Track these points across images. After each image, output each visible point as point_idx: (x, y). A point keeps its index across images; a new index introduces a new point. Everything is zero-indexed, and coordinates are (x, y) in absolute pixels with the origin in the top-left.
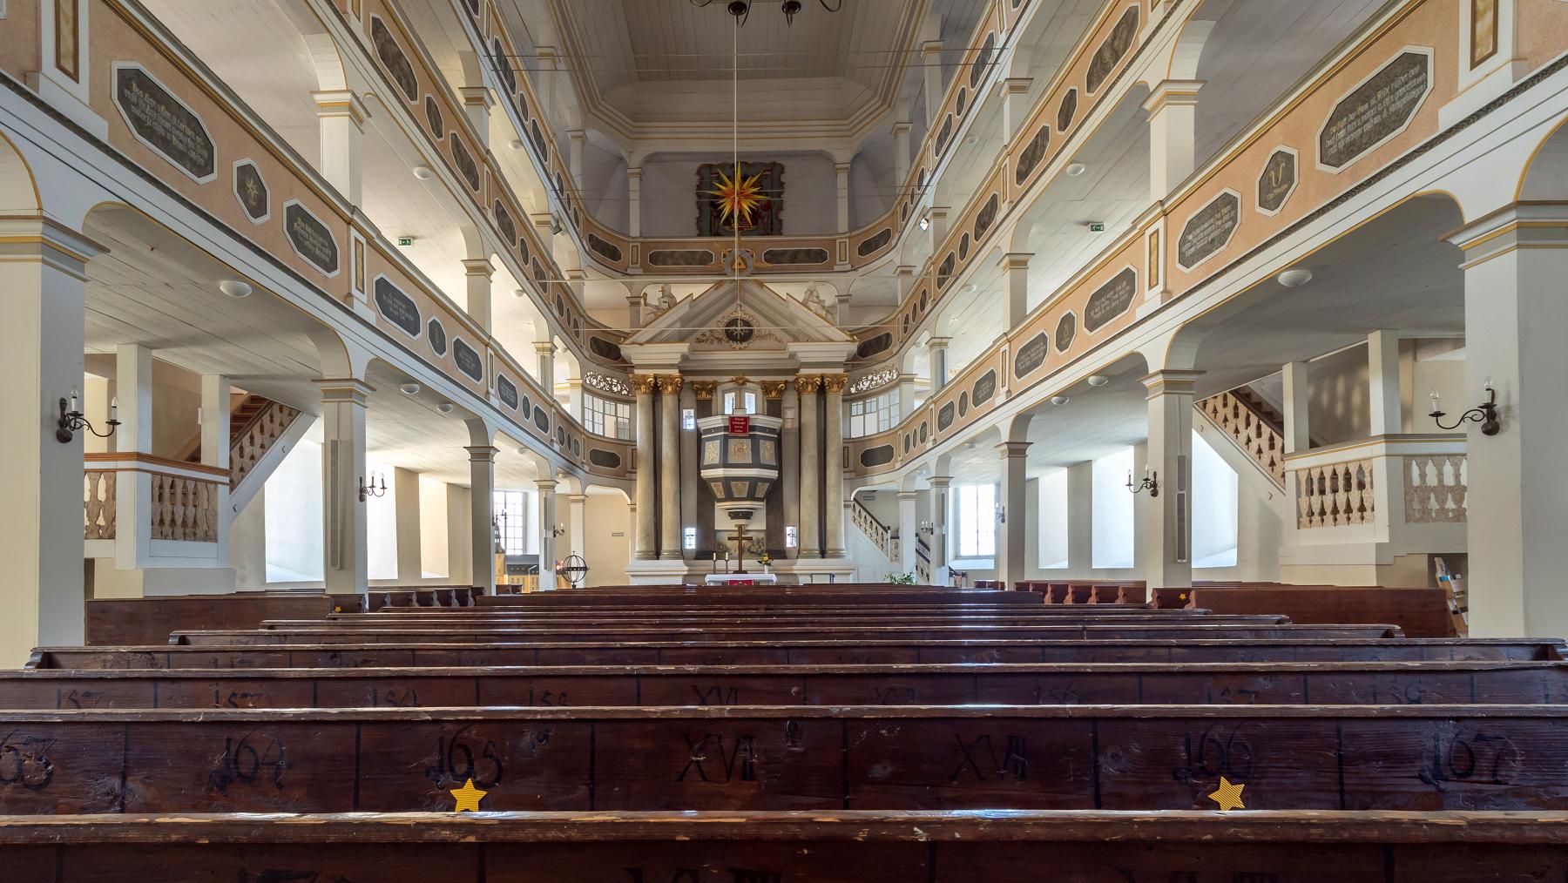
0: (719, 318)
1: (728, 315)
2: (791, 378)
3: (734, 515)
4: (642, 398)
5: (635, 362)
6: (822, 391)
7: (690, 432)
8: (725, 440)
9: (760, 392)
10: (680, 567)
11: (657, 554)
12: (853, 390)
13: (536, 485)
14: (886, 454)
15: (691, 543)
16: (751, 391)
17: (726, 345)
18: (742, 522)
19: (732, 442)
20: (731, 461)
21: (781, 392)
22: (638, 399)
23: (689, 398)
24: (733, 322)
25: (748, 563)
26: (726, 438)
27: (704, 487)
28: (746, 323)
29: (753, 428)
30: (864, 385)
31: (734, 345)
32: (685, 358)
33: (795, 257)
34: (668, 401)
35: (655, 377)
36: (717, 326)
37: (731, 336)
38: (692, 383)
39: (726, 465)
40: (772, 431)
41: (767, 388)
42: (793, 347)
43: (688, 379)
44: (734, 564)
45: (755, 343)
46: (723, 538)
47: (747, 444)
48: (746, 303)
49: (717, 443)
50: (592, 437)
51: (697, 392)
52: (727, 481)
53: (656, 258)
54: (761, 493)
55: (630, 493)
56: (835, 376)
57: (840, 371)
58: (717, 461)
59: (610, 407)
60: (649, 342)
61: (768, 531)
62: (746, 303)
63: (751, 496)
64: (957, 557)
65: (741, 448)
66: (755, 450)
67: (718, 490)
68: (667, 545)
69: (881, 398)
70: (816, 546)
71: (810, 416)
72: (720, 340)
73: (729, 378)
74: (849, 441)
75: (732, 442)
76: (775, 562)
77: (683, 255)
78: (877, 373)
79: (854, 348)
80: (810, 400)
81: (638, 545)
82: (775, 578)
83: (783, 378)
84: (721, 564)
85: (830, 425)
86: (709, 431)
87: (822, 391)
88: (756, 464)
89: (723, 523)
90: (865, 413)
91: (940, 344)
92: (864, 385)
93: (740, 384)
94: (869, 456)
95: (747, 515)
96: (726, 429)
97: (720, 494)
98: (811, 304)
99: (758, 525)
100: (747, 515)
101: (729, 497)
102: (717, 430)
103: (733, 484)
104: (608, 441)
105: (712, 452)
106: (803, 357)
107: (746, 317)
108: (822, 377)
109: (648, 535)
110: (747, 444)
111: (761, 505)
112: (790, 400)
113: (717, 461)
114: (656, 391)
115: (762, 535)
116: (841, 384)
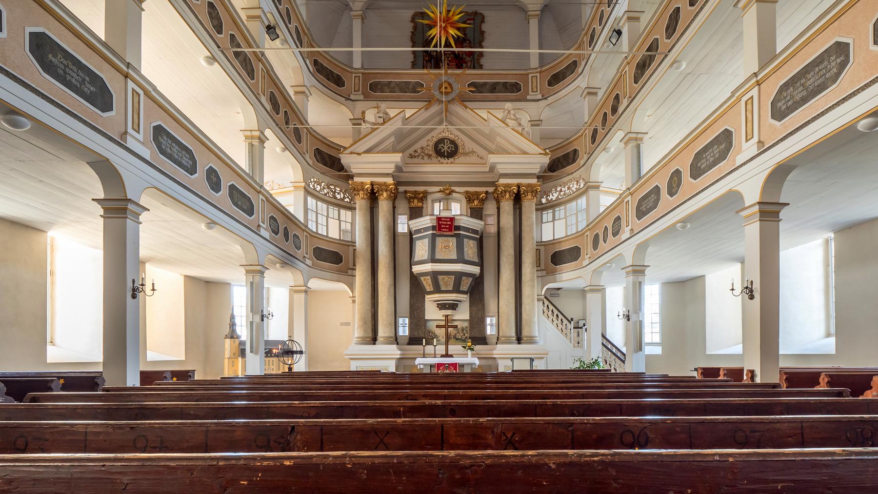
0: (429, 137)
1: (435, 136)
2: (491, 189)
3: (442, 306)
4: (361, 203)
5: (354, 171)
6: (518, 199)
8: (433, 238)
9: (464, 201)
10: (394, 351)
11: (374, 340)
12: (544, 201)
14: (574, 254)
15: (404, 331)
16: (456, 200)
17: (435, 160)
18: (449, 312)
20: (438, 257)
21: (482, 201)
22: (357, 206)
23: (402, 206)
24: (441, 141)
25: (454, 348)
27: (415, 280)
28: (453, 142)
29: (458, 228)
30: (553, 196)
31: (442, 160)
32: (399, 169)
33: (494, 88)
34: (384, 205)
35: (372, 184)
36: (427, 142)
37: (439, 153)
38: (406, 192)
40: (475, 232)
41: (470, 198)
42: (493, 159)
43: (401, 189)
44: (441, 349)
45: (460, 159)
46: (432, 326)
47: (452, 242)
49: (426, 241)
51: (409, 200)
52: (435, 275)
53: (374, 87)
54: (465, 286)
55: (351, 287)
56: (529, 185)
57: (534, 181)
58: (426, 257)
59: (333, 211)
60: (368, 151)
61: (471, 321)
63: (457, 290)
65: (447, 246)
66: (460, 248)
68: (383, 331)
69: (569, 206)
70: (514, 334)
71: (508, 220)
72: (430, 156)
73: (437, 189)
74: (540, 243)
76: (478, 348)
77: (398, 84)
78: (565, 184)
79: (546, 160)
80: (507, 206)
81: (357, 331)
82: (477, 361)
83: (484, 189)
84: (429, 349)
85: (525, 228)
86: (418, 231)
87: (518, 199)
88: (461, 260)
89: (433, 313)
90: (554, 219)
91: (636, 139)
92: (553, 196)
93: (448, 193)
94: (557, 257)
95: (453, 306)
96: (434, 228)
98: (508, 121)
99: (463, 315)
100: (453, 306)
101: (437, 290)
102: (426, 229)
103: (440, 277)
104: (332, 241)
105: (422, 249)
106: (501, 169)
107: (451, 137)
108: (519, 186)
109: (365, 323)
110: (452, 242)
111: (465, 298)
112: (490, 208)
113: (426, 257)
114: (373, 197)
116: (535, 192)
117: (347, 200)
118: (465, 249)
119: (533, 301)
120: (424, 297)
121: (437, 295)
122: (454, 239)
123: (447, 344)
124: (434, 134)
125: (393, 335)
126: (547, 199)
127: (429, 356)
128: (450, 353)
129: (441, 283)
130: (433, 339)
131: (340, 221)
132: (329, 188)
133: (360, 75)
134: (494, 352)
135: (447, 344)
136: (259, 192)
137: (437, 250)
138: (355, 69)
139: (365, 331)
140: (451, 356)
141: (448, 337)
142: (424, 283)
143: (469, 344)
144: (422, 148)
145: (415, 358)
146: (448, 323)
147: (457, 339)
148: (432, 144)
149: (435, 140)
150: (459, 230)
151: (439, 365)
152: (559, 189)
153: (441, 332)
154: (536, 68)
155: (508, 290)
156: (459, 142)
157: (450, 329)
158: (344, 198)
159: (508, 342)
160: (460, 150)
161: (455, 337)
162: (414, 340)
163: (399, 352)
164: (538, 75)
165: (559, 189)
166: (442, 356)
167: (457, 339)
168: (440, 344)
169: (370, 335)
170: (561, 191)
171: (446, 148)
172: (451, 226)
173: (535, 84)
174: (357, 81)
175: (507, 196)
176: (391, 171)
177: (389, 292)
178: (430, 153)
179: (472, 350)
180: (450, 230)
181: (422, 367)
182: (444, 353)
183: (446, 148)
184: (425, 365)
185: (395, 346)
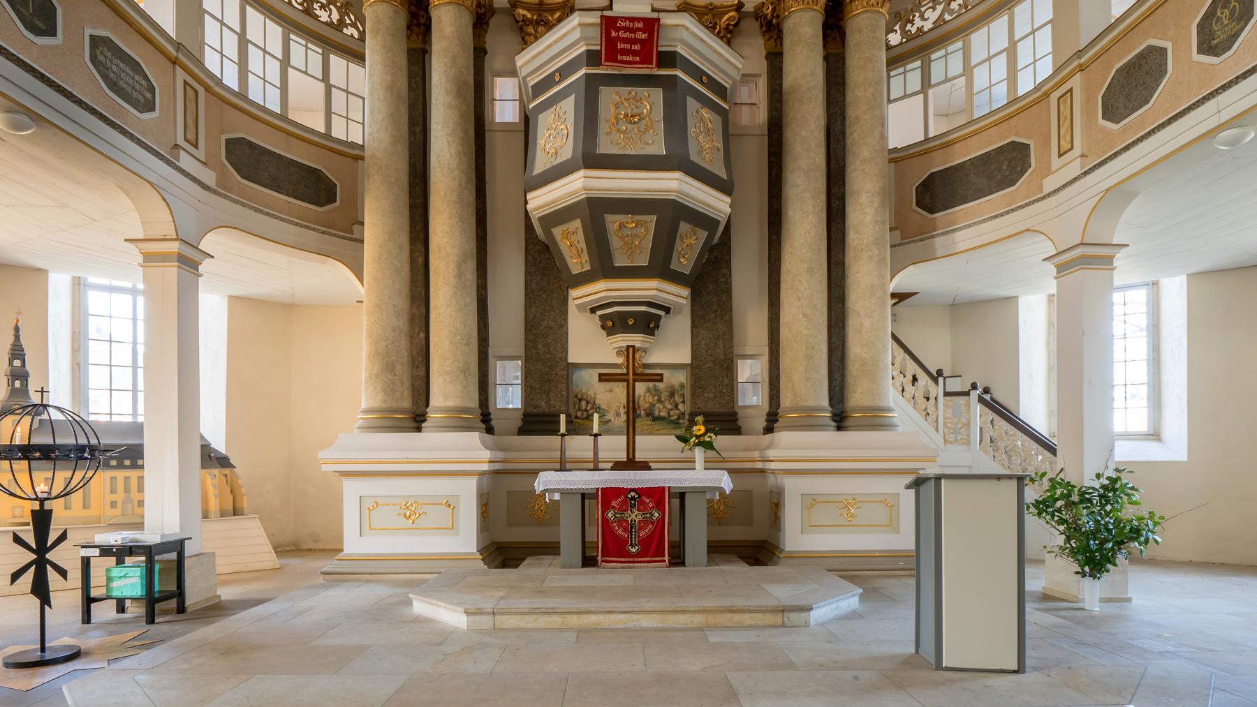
7: (507, 128)
13: (134, 255)
14: (1005, 166)
18: (637, 339)
19: (609, 97)
25: (651, 444)
39: (592, 159)
44: (613, 446)
50: (237, 103)
54: (684, 262)
64: (1155, 435)
69: (978, 38)
70: (822, 399)
75: (609, 97)
76: (721, 441)
84: (579, 445)
90: (926, 84)
94: (936, 190)
95: (646, 321)
97: (577, 262)
100: (646, 321)
102: (565, 71)
104: (302, 135)
109: (389, 368)
111: (677, 295)
115: (680, 378)
118: (692, 130)
120: (565, 301)
121: (601, 285)
123: (631, 431)
125: (474, 403)
126: (904, 33)
128: (639, 456)
130: (589, 418)
131: (329, 88)
134: (771, 454)
135: (631, 431)
136: (175, 62)
137: (603, 127)
139: (389, 390)
140: (645, 466)
141: (632, 407)
143: (699, 429)
145: (535, 473)
146: (633, 372)
151: (609, 495)
153: (612, 397)
157: (640, 388)
158: (341, 23)
159: (807, 423)
161: (649, 414)
162: (536, 422)
163: (487, 454)
166: (618, 466)
168: (610, 432)
169: (407, 403)
172: (648, 45)
177: (459, 275)
179: (709, 446)
181: (557, 497)
182: (623, 456)
184: (564, 493)
185: (474, 438)
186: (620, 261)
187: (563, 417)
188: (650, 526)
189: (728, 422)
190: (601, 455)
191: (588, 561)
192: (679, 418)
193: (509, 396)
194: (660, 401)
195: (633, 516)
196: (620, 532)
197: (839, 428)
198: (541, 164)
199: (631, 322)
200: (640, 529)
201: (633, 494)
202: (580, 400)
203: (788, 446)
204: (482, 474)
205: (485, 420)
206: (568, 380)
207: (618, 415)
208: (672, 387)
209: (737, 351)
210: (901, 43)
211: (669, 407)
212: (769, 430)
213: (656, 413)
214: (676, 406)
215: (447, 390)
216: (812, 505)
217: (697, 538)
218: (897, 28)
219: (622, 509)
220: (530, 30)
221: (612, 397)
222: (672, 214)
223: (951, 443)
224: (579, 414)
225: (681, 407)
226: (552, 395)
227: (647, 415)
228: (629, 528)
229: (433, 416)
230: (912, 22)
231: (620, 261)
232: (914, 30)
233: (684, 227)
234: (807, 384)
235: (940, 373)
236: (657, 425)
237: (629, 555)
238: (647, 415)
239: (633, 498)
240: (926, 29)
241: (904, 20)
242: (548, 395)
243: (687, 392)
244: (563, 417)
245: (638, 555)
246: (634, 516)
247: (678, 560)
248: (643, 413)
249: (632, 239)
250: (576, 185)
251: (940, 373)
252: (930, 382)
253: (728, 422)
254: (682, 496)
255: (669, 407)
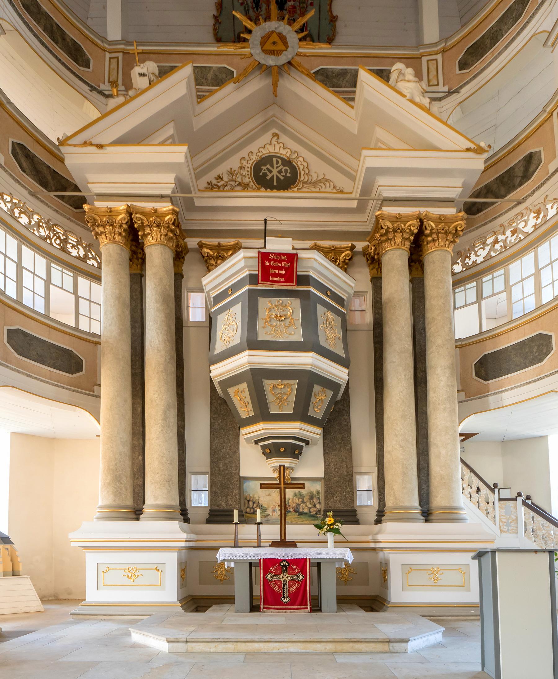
3: (272, 450)
4: (111, 252)
7: (198, 325)
18: (287, 462)
20: (262, 335)
24: (267, 160)
25: (297, 530)
26: (253, 296)
28: (288, 163)
29: (305, 280)
30: (479, 256)
34: (157, 256)
35: (130, 212)
36: (241, 161)
44: (271, 532)
46: (253, 489)
47: (294, 306)
48: (284, 131)
52: (256, 377)
54: (318, 409)
59: (62, 277)
61: (327, 480)
62: (284, 131)
63: (301, 414)
65: (282, 317)
66: (309, 320)
67: (241, 400)
70: (416, 503)
76: (345, 529)
82: (349, 556)
84: (248, 531)
88: (310, 344)
89: (254, 465)
90: (480, 297)
92: (479, 256)
96: (252, 279)
99: (311, 468)
100: (294, 449)
101: (263, 414)
103: (268, 384)
105: (230, 328)
106: (387, 186)
107: (285, 153)
109: (117, 479)
110: (294, 306)
111: (314, 433)
115: (317, 487)
117: (91, 262)
119: (455, 440)
120: (237, 436)
122: (297, 303)
123: (283, 522)
124: (254, 147)
125: (175, 501)
126: (464, 265)
127: (247, 543)
128: (289, 538)
129: (270, 398)
130: (255, 513)
132: (50, 228)
133: (120, 55)
135: (283, 522)
138: (111, 43)
139: (117, 493)
140: (293, 545)
141: (284, 506)
142: (236, 400)
143: (330, 520)
144: (231, 173)
145: (217, 549)
146: (284, 483)
147: (301, 514)
148: (249, 165)
149: (255, 158)
150: (308, 284)
151: (268, 563)
152: (490, 241)
153: (270, 499)
154: (435, 44)
155: (404, 417)
156: (300, 164)
157: (289, 493)
159: (404, 516)
160: (302, 177)
161: (296, 510)
162: (218, 515)
163: (184, 536)
164: (439, 57)
165: (490, 241)
166: (274, 544)
167: (301, 514)
168: (268, 522)
169: (129, 502)
170: (496, 242)
171: (275, 172)
173: (433, 73)
174: (114, 65)
175: (399, 240)
176: (167, 191)
177: (165, 419)
178: (246, 180)
179: (337, 531)
180: (289, 280)
181: (232, 565)
182: (278, 538)
183: (275, 172)
184: (237, 562)
185: (176, 525)
186: (274, 410)
187: (236, 512)
188: (297, 585)
189: (350, 516)
190: (263, 537)
191: (254, 608)
192: (316, 513)
193: (199, 499)
194: (303, 502)
195: (285, 578)
196: (276, 588)
197: (426, 521)
198: (219, 347)
199: (282, 450)
200: (290, 586)
201: (285, 563)
202: (249, 501)
203: (391, 532)
204: (181, 549)
205: (184, 514)
206: (240, 487)
207: (274, 511)
208: (312, 493)
209: (355, 469)
210: (462, 271)
211: (310, 506)
212: (378, 521)
213: (301, 510)
214: (314, 506)
215: (157, 493)
216: (409, 572)
217: (330, 591)
218: (459, 261)
219: (277, 574)
220: (213, 262)
221: (270, 499)
222: (308, 380)
223: (505, 532)
224: (248, 510)
225: (318, 506)
226: (229, 497)
227: (295, 511)
228: (283, 586)
229: (148, 510)
230: (469, 257)
231: (274, 410)
232: (470, 263)
233: (317, 388)
234: (403, 491)
235: (495, 486)
236: (302, 518)
237: (282, 604)
238: (295, 511)
239: (285, 566)
240: (478, 262)
241: (464, 256)
242: (226, 498)
243: (322, 496)
244: (236, 512)
245: (288, 604)
246: (286, 578)
247: (317, 607)
248: (292, 510)
249: (282, 395)
250: (243, 361)
251: (495, 486)
252: (489, 492)
253: (350, 516)
254: (319, 564)
255: (310, 506)
